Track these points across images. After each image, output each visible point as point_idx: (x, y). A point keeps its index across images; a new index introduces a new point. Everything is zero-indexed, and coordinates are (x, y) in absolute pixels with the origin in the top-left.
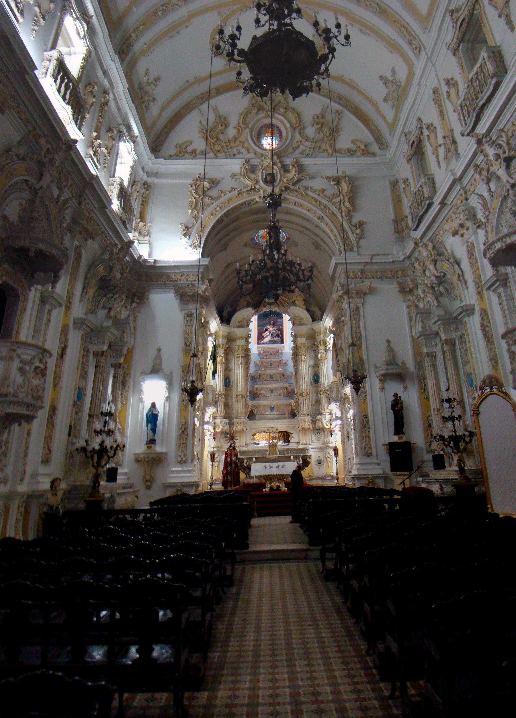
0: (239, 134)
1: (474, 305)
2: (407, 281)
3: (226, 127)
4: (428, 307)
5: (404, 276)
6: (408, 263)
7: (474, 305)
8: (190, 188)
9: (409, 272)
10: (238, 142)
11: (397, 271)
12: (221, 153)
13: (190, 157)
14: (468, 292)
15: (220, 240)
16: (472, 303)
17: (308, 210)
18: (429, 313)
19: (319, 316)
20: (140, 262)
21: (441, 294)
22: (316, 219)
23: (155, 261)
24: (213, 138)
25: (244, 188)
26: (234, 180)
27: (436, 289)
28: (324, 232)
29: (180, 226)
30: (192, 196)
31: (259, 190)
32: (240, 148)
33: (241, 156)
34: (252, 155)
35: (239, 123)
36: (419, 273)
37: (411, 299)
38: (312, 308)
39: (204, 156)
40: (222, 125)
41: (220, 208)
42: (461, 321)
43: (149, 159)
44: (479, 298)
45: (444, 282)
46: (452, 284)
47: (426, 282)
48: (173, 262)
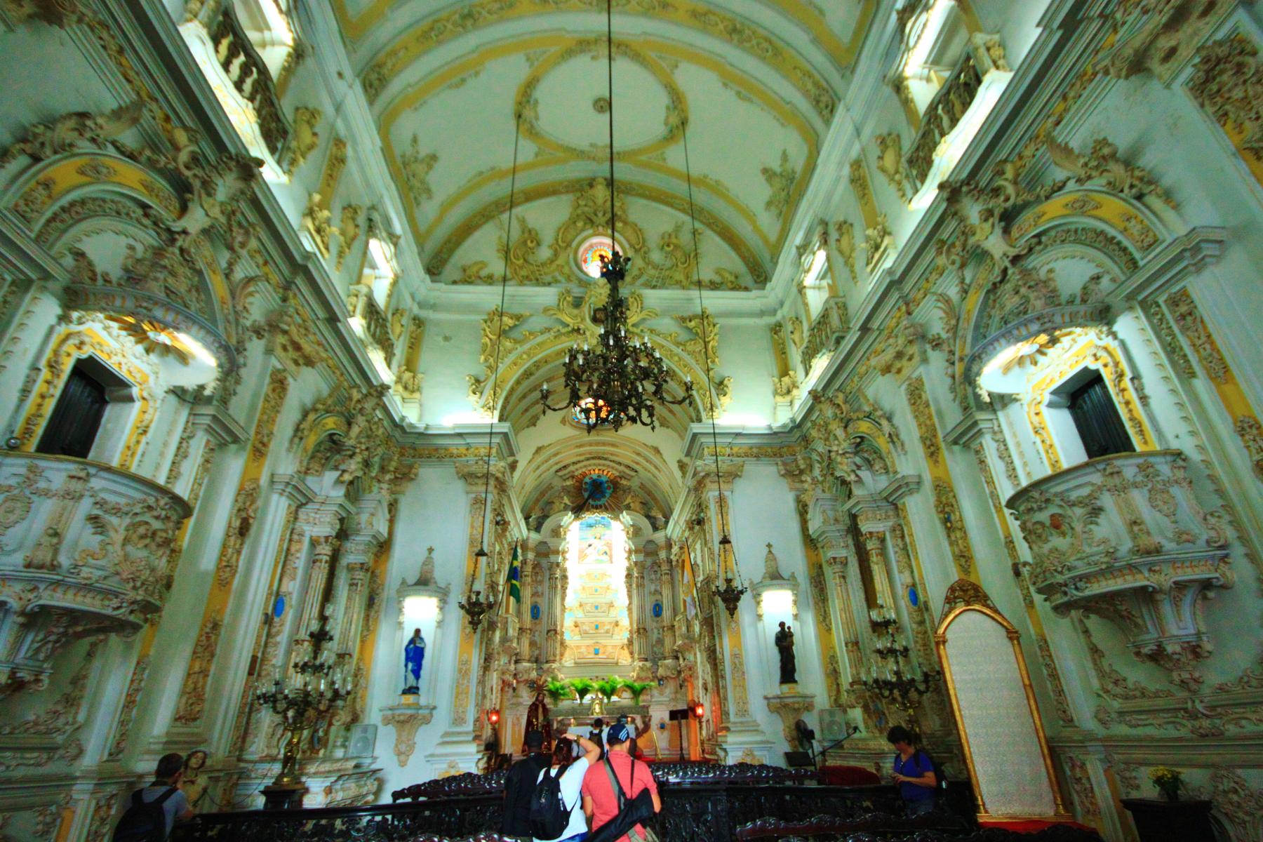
0: (556, 254)
3: (538, 244)
8: (484, 325)
10: (554, 266)
15: (526, 410)
23: (427, 427)
35: (557, 240)
38: (653, 513)
43: (423, 281)
45: (862, 450)
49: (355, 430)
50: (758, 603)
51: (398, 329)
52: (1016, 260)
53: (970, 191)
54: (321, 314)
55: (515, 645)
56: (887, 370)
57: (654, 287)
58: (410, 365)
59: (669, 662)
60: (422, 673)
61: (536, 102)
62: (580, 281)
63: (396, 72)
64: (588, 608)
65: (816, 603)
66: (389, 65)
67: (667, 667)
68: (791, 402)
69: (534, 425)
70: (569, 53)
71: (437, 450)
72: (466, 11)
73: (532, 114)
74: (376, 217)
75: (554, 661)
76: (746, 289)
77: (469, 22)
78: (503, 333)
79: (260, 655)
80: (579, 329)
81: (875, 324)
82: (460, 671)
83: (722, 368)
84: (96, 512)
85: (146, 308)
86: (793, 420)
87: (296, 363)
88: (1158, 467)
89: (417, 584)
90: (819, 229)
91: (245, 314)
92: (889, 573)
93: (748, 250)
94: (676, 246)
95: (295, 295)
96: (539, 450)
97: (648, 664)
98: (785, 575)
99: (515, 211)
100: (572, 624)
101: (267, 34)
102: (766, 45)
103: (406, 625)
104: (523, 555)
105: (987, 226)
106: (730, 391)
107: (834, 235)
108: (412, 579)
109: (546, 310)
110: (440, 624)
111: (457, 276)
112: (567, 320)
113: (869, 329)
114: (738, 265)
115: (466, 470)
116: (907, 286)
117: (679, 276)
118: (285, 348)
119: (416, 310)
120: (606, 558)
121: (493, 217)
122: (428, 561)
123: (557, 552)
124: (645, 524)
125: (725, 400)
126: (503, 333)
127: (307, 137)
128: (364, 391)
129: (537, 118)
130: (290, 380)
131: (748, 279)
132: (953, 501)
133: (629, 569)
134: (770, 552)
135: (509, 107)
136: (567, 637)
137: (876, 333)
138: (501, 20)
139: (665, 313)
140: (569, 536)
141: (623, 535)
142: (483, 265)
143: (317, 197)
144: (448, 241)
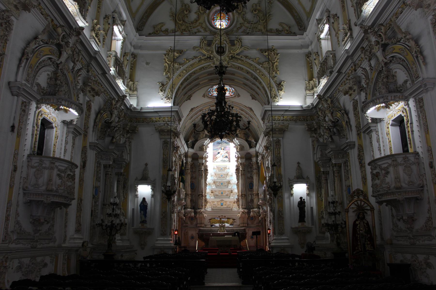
0: (199, 17)
1: (355, 142)
3: (190, 12)
4: (325, 141)
5: (312, 120)
6: (315, 111)
7: (355, 142)
8: (165, 57)
10: (197, 24)
11: (307, 117)
12: (187, 31)
14: (352, 133)
15: (186, 93)
16: (354, 141)
17: (248, 73)
19: (254, 144)
20: (131, 109)
21: (334, 134)
22: (253, 79)
23: (141, 108)
24: (180, 21)
25: (203, 56)
27: (331, 130)
28: (258, 88)
29: (158, 84)
31: (213, 59)
32: (199, 27)
33: (200, 34)
34: (207, 33)
37: (315, 136)
38: (250, 139)
39: (174, 34)
40: (187, 11)
41: (186, 71)
46: (342, 127)
47: (325, 126)
49: (114, 116)
51: (126, 62)
52: (386, 64)
53: (371, 32)
54: (100, 72)
56: (346, 93)
57: (248, 34)
58: (132, 78)
60: (147, 215)
62: (211, 31)
64: (218, 184)
65: (317, 189)
67: (254, 212)
68: (313, 94)
74: (116, 15)
75: (202, 208)
76: (295, 34)
78: (174, 60)
79: (93, 209)
80: (210, 57)
83: (281, 76)
84: (59, 173)
85: (60, 102)
86: (312, 104)
87: (94, 96)
88: (409, 158)
90: (326, 15)
91: (78, 84)
92: (341, 180)
93: (296, 12)
94: (259, 11)
95: (91, 68)
96: (192, 109)
97: (246, 211)
100: (210, 192)
103: (139, 196)
104: (186, 160)
105: (377, 47)
106: (284, 88)
107: (332, 20)
109: (194, 48)
110: (153, 196)
111: (151, 31)
112: (205, 52)
113: (341, 72)
114: (291, 21)
115: (160, 129)
116: (355, 58)
118: (90, 92)
119: (133, 50)
120: (226, 159)
123: (202, 158)
125: (282, 93)
126: (174, 60)
128: (117, 99)
130: (92, 104)
131: (295, 29)
132: (363, 155)
136: (208, 197)
137: (344, 75)
139: (253, 47)
142: (163, 24)
144: (146, 12)
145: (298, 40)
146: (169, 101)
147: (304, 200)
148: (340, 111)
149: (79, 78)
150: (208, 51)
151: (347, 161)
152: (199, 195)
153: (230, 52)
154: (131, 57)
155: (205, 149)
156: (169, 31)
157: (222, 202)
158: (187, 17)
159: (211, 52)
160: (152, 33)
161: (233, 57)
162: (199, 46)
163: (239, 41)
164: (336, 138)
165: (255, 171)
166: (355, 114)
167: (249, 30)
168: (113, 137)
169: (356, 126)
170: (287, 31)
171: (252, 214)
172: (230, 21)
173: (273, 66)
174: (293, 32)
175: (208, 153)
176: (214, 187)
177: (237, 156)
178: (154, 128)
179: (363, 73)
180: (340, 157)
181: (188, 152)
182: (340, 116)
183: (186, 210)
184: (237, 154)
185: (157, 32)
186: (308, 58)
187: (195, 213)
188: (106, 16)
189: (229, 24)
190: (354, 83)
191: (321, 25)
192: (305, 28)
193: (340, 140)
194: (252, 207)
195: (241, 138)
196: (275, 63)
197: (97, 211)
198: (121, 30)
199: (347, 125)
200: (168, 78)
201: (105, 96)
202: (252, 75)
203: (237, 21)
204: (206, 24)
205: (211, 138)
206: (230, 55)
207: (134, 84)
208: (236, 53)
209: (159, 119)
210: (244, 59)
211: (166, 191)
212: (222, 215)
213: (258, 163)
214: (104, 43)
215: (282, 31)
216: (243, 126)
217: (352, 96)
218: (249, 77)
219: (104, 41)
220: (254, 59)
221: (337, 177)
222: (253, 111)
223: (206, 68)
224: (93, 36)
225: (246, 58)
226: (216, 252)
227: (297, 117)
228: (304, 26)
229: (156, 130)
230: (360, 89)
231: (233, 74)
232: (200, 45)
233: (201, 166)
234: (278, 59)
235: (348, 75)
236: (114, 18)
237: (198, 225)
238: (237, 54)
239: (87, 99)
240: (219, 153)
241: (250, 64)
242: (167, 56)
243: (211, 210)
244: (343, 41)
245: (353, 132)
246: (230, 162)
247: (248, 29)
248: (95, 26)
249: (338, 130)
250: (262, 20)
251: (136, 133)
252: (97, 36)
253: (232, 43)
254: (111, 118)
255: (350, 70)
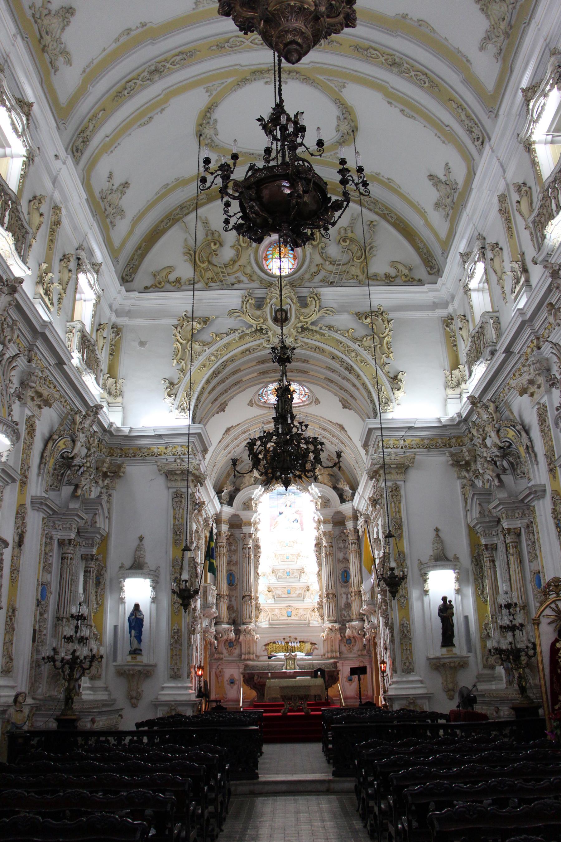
0: (238, 255)
1: (544, 485)
2: (462, 451)
3: (221, 245)
4: (487, 486)
5: (459, 445)
6: (465, 428)
7: (544, 485)
9: (466, 440)
10: (236, 267)
11: (450, 439)
12: (215, 282)
13: (173, 288)
14: (538, 469)
15: (216, 400)
16: (543, 483)
18: (490, 494)
19: (349, 495)
21: (504, 470)
23: (131, 430)
24: (203, 263)
26: (233, 318)
27: (498, 463)
28: (354, 386)
29: (163, 382)
30: (178, 341)
32: (239, 274)
33: (241, 286)
34: (256, 285)
36: (478, 441)
37: (467, 475)
38: (340, 486)
39: (192, 287)
40: (215, 244)
41: (217, 357)
42: (528, 506)
44: (552, 477)
45: (509, 454)
46: (519, 458)
47: (485, 455)
48: (154, 430)
49: (78, 444)
50: (425, 581)
51: (101, 342)
54: (52, 361)
55: (214, 610)
56: (523, 391)
57: (332, 284)
58: (112, 373)
59: (355, 623)
60: (143, 637)
61: (216, 121)
62: (261, 281)
63: (96, 129)
64: (280, 574)
65: (476, 580)
66: (91, 127)
67: (352, 627)
68: (461, 394)
69: (223, 410)
70: (243, 81)
71: (140, 449)
72: (153, 68)
73: (212, 132)
76: (420, 282)
77: (156, 77)
78: (193, 338)
79: (37, 628)
80: (262, 329)
81: (516, 349)
82: (173, 637)
86: (459, 415)
87: (40, 407)
89: (131, 568)
90: (477, 245)
91: (11, 385)
92: (521, 562)
93: (422, 242)
94: (352, 240)
95: (36, 354)
96: (228, 430)
97: (337, 626)
98: (450, 555)
99: (200, 211)
100: (266, 589)
101: (8, 150)
102: (423, 77)
103: (127, 600)
104: (217, 528)
106: (403, 385)
107: (489, 255)
108: (128, 564)
109: (231, 313)
110: (154, 600)
113: (512, 352)
115: (166, 468)
116: (538, 323)
117: (355, 271)
118: (32, 399)
119: (114, 319)
121: (178, 220)
122: (139, 548)
123: (249, 524)
124: (333, 496)
125: (399, 394)
126: (193, 338)
127: (36, 219)
128: (84, 413)
129: (216, 134)
130: (37, 421)
131: (421, 272)
133: (317, 538)
134: (437, 535)
135: (191, 128)
136: (261, 601)
137: (517, 356)
138: (183, 67)
139: (342, 309)
140: (260, 508)
141: (313, 505)
142: (171, 269)
143: (44, 266)
144: (139, 248)
145: (427, 293)
146: (183, 414)
147: (450, 601)
148: (514, 427)
149: (13, 373)
150: (256, 318)
151: (532, 522)
152: (244, 597)
153: (299, 318)
154: (111, 331)
155: (254, 505)
156: (182, 281)
157: (289, 610)
158: (217, 255)
159: (262, 321)
160: (151, 287)
161: (303, 329)
162: (239, 308)
163: (316, 298)
164: (508, 479)
165: (352, 547)
166: (542, 431)
167: (335, 277)
168: (77, 486)
169: (545, 455)
170: (406, 276)
171: (348, 632)
172: (297, 261)
173: (381, 343)
174: (417, 278)
175: (259, 514)
176: (273, 580)
177: (316, 519)
178: (156, 467)
179: (554, 351)
180: (517, 515)
181: (221, 512)
182: (513, 436)
183: (219, 627)
184: (318, 515)
185: (160, 283)
186: (447, 326)
187: (238, 632)
188: (64, 256)
189: (295, 266)
190: (537, 372)
191: (470, 264)
192: (439, 271)
193: (515, 483)
194: (348, 618)
195: (325, 484)
196: (384, 337)
197: (45, 632)
198: (92, 283)
199: (528, 452)
200: (182, 371)
201: (62, 407)
202: (342, 362)
203: (311, 261)
204: (252, 268)
205: (266, 485)
206: (300, 325)
207: (116, 383)
208: (310, 320)
209: (164, 451)
210: (326, 331)
211: (180, 590)
212: (289, 635)
213: (358, 531)
214: (61, 306)
215: (396, 276)
216: (328, 459)
217: (536, 396)
218: (335, 365)
219: (60, 303)
220: (344, 332)
221: (513, 555)
222: (346, 431)
223: (253, 350)
224: (40, 294)
225: (330, 329)
226: (279, 711)
227: (430, 440)
228: (436, 266)
229: (160, 470)
230: (551, 383)
231: (306, 361)
232: (242, 307)
233: (247, 539)
234: (390, 331)
235: (524, 357)
236: (79, 259)
237: (243, 657)
238: (312, 324)
239: (28, 412)
240: (281, 513)
241: (337, 340)
242: (179, 329)
243: (267, 626)
244: (513, 292)
245: (539, 466)
246: (302, 529)
247: (332, 275)
248: (44, 275)
249: (511, 464)
250: (359, 258)
251: (120, 477)
252: (47, 292)
253: (303, 302)
254: (73, 448)
255: (528, 347)
